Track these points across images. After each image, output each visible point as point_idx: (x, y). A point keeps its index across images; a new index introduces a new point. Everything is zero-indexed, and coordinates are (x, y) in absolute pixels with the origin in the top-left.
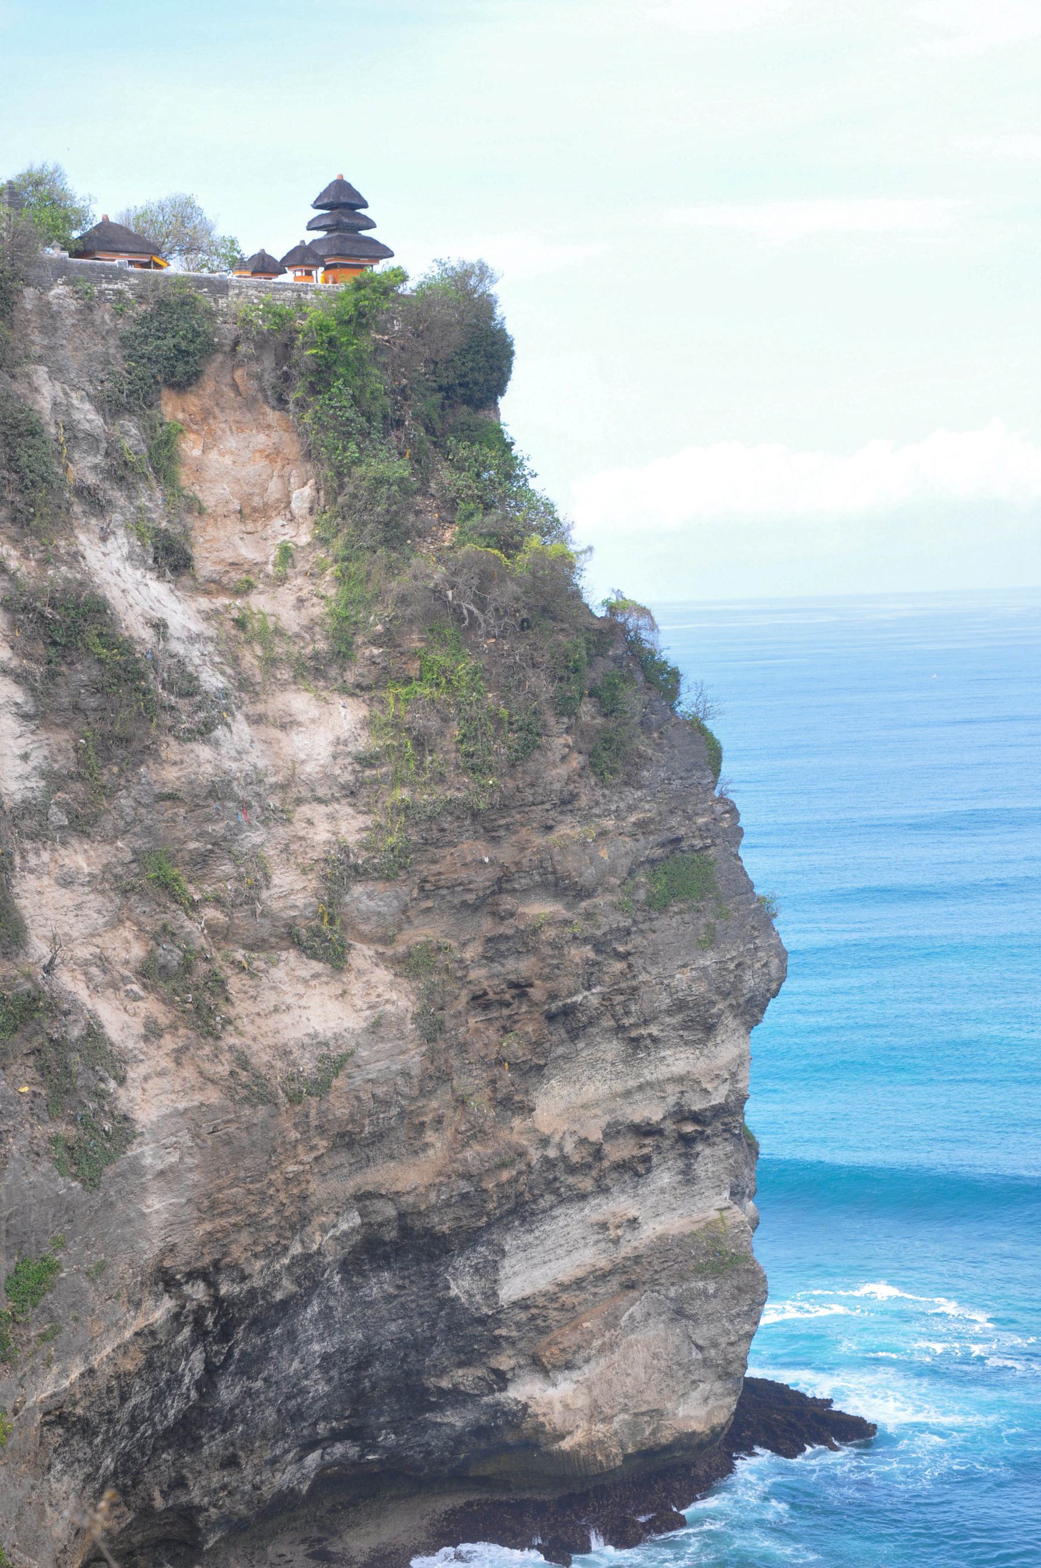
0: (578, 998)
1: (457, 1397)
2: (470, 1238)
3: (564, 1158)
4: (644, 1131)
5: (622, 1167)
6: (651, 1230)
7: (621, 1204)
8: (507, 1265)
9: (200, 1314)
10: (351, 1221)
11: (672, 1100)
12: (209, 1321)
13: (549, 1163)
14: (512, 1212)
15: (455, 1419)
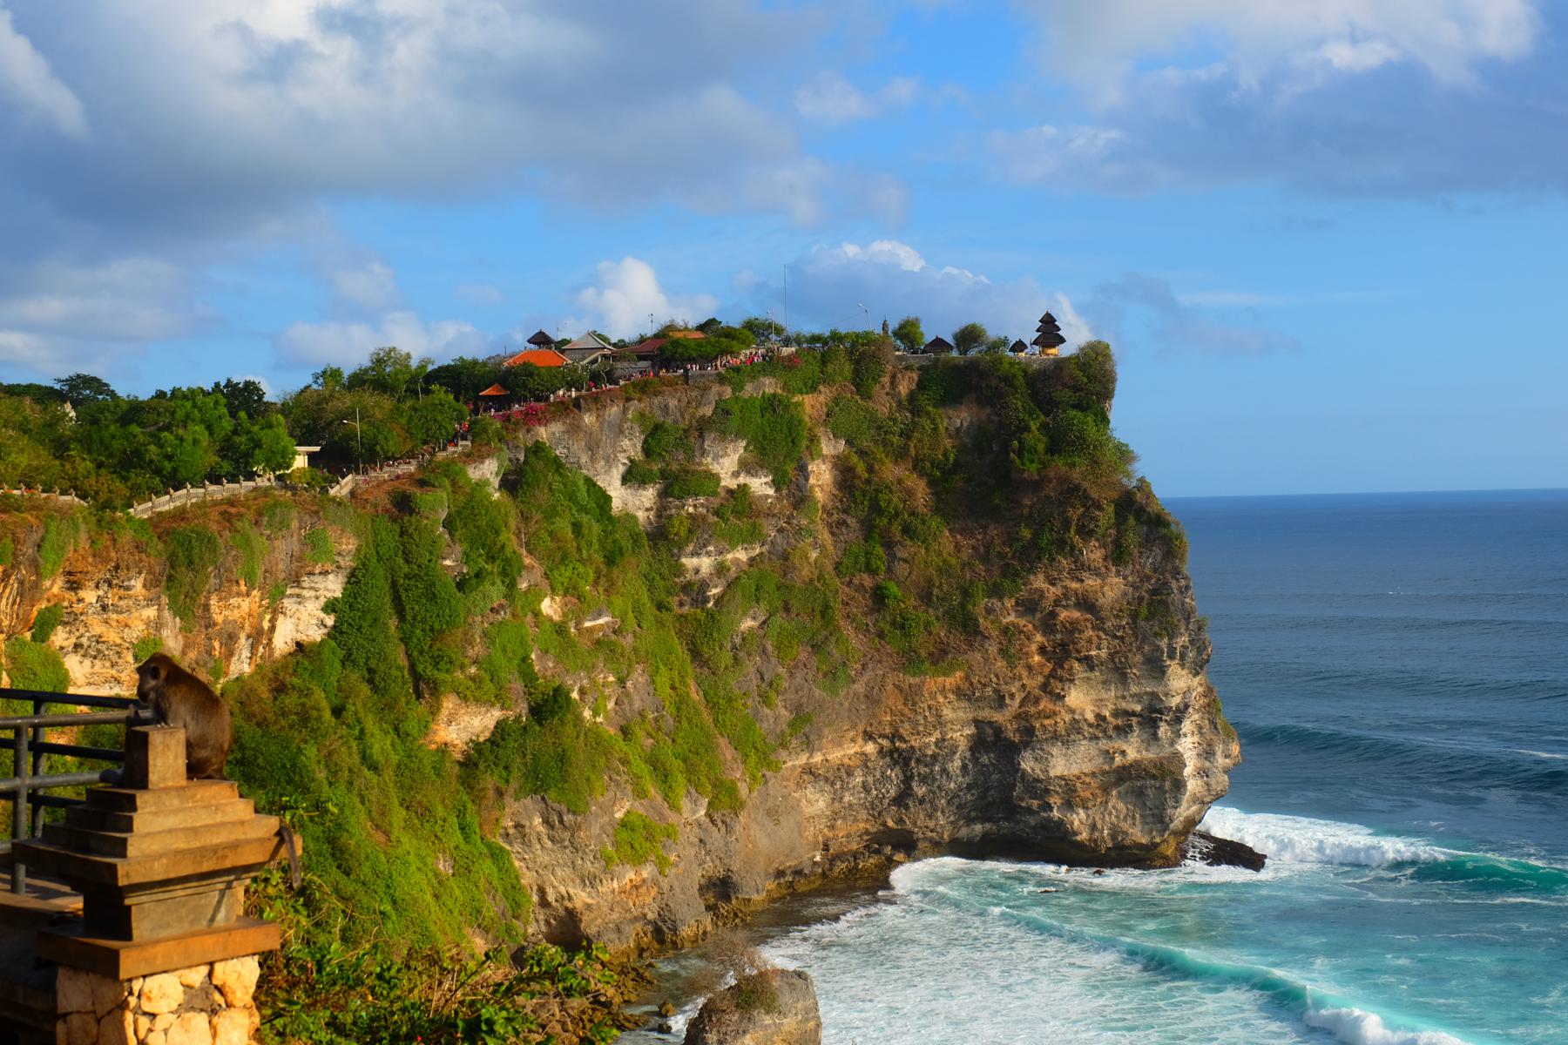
0: (1093, 653)
1: (1030, 811)
2: (1026, 745)
4: (1134, 714)
5: (1117, 728)
6: (1132, 755)
7: (1119, 744)
8: (1053, 761)
9: (891, 753)
10: (970, 731)
13: (1077, 721)
15: (1032, 821)
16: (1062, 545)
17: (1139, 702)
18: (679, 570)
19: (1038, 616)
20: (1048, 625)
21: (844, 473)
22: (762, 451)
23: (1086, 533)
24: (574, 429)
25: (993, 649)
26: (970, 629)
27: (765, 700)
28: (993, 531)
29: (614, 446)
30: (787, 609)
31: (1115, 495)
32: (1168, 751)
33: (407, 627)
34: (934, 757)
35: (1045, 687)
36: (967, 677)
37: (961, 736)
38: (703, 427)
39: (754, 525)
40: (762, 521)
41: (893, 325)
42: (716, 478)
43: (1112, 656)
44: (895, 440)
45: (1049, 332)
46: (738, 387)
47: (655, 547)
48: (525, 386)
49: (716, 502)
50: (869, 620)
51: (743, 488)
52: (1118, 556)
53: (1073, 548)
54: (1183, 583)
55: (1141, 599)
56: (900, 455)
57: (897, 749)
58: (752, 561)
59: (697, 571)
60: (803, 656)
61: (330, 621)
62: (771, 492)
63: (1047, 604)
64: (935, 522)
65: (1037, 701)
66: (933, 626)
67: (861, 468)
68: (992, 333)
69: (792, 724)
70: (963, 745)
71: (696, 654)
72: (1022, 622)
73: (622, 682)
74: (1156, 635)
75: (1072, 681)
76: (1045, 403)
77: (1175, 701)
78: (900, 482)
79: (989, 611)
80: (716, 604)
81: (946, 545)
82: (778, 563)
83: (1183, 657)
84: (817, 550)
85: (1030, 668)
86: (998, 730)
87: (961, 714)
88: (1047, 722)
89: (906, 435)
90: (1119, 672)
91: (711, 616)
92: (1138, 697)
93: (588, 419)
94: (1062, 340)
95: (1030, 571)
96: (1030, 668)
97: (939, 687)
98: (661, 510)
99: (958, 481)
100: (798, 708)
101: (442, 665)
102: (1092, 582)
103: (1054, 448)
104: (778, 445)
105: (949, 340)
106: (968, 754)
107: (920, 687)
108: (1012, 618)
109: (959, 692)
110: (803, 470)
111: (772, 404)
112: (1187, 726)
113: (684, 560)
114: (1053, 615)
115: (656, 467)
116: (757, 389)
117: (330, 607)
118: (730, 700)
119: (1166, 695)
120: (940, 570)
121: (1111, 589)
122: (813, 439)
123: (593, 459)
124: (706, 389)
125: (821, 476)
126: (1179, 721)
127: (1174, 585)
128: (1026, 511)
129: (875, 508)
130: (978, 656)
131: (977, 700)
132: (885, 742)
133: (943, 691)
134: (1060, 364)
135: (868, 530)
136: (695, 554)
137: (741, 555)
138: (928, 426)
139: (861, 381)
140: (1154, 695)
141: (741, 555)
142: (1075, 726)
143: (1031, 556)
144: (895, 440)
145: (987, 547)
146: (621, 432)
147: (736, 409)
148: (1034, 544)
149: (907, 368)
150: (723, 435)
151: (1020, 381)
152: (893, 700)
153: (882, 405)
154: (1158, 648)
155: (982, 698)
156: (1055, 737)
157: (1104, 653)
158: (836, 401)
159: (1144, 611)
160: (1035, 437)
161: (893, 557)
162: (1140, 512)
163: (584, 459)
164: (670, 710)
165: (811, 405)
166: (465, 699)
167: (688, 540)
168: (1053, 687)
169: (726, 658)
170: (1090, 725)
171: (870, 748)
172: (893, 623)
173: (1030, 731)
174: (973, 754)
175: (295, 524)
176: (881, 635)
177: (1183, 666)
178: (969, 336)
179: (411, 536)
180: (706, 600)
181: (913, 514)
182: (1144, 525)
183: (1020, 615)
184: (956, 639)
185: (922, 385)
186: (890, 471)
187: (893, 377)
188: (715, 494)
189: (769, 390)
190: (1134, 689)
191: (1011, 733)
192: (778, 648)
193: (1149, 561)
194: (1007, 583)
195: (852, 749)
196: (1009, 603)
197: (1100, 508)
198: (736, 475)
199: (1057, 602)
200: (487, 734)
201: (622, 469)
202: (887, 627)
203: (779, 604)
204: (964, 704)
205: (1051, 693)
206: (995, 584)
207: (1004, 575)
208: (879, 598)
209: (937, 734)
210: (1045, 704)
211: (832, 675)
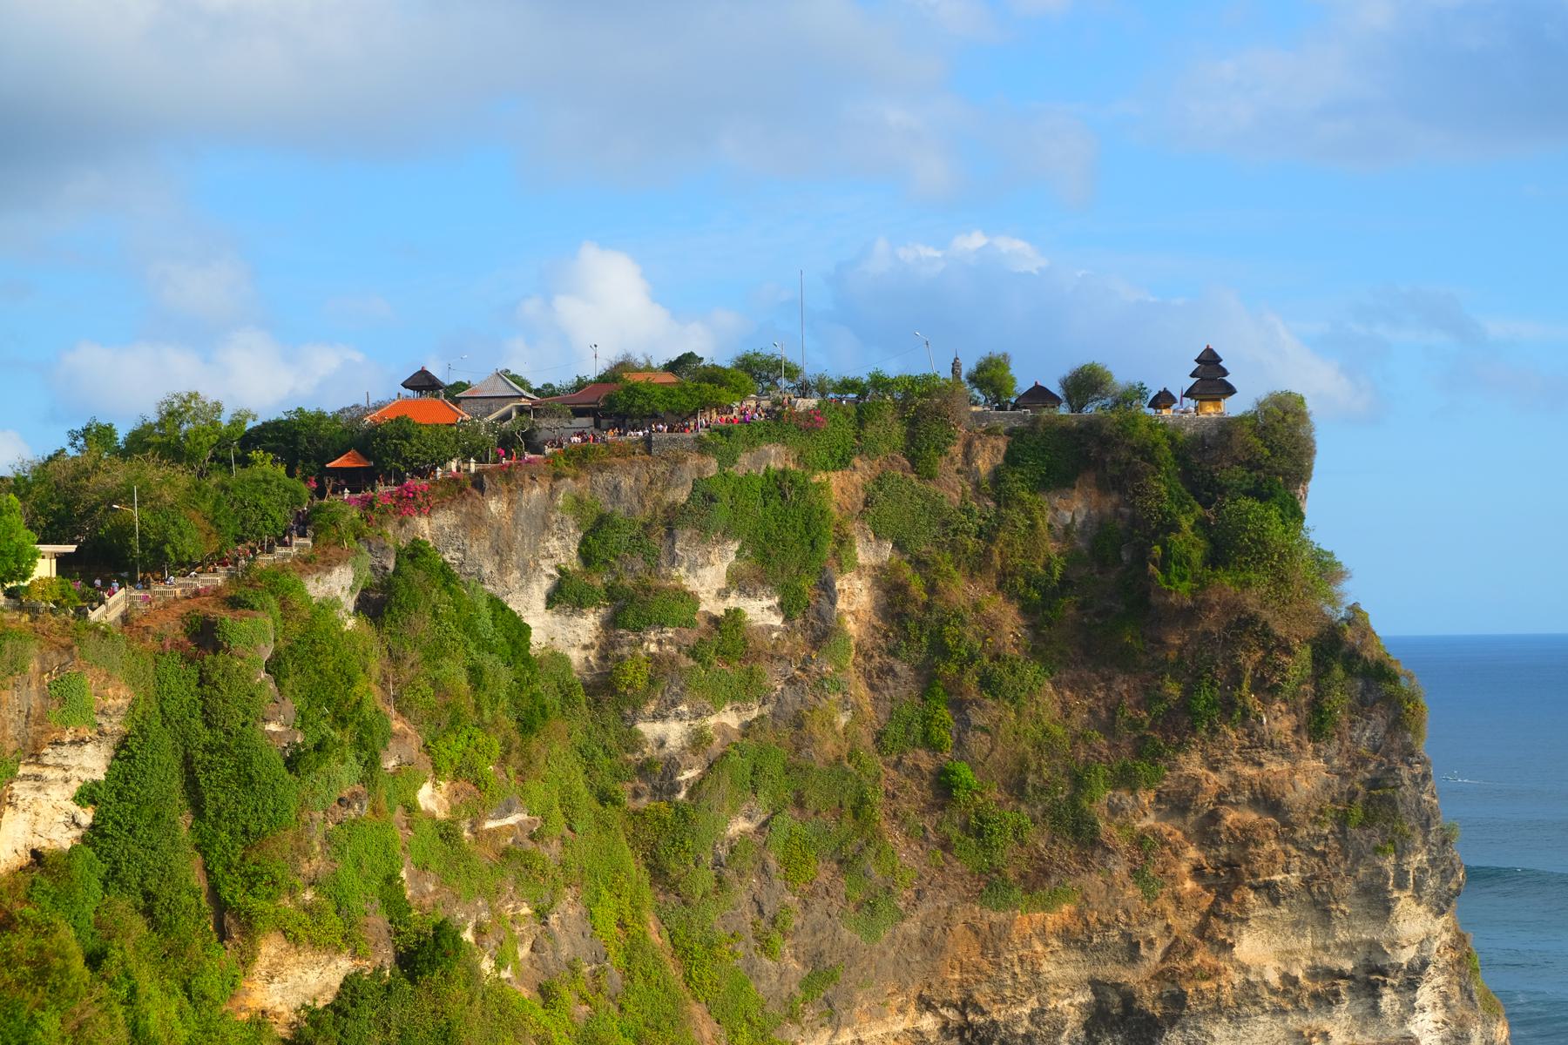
0: (1278, 878)
2: (1173, 1021)
3: (1266, 983)
4: (1341, 975)
5: (1315, 996)
7: (1318, 1021)
9: (961, 1030)
10: (1084, 997)
11: (1362, 957)
12: (968, 1035)
14: (1213, 1011)
16: (1228, 707)
17: (1350, 955)
18: (633, 741)
19: (1192, 818)
20: (1207, 831)
21: (891, 592)
22: (765, 558)
23: (1266, 689)
24: (474, 522)
25: (1120, 869)
26: (1083, 836)
27: (765, 946)
28: (1121, 685)
29: (535, 549)
30: (800, 803)
31: (1312, 631)
32: (1396, 1032)
33: (206, 827)
34: (1028, 1037)
35: (1202, 930)
36: (1080, 913)
37: (1071, 1005)
38: (672, 520)
39: (750, 673)
40: (763, 667)
41: (968, 366)
42: (692, 599)
43: (1307, 883)
44: (970, 543)
45: (1211, 377)
46: (728, 459)
47: (596, 705)
48: (397, 455)
49: (691, 636)
50: (928, 822)
51: (734, 615)
52: (1316, 725)
53: (1246, 714)
54: (1418, 769)
55: (1353, 794)
56: (978, 566)
57: (970, 1025)
58: (747, 728)
59: (661, 743)
60: (824, 877)
61: (86, 817)
62: (777, 621)
63: (1206, 801)
64: (1031, 671)
65: (1189, 952)
66: (1025, 830)
67: (917, 586)
68: (1122, 376)
69: (807, 984)
70: (1073, 1019)
71: (658, 873)
72: (1166, 828)
73: (542, 915)
74: (1377, 850)
75: (1244, 921)
76: (1204, 488)
77: (1406, 956)
78: (977, 607)
79: (1114, 810)
80: (691, 794)
81: (1045, 709)
82: (786, 733)
83: (1418, 885)
84: (846, 714)
85: (1178, 900)
86: (1128, 998)
87: (1070, 971)
88: (1205, 985)
89: (987, 535)
90: (1322, 911)
91: (682, 813)
92: (1348, 948)
93: (495, 506)
94: (1230, 390)
95: (1179, 748)
96: (1178, 900)
97: (1036, 927)
98: (607, 649)
99: (1067, 607)
100: (815, 959)
101: (260, 888)
102: (1275, 767)
103: (1218, 557)
104: (789, 548)
105: (1055, 388)
106: (1081, 1034)
107: (1006, 927)
108: (1150, 821)
109: (1067, 937)
110: (826, 588)
111: (779, 485)
112: (1425, 995)
113: (642, 726)
114: (1214, 817)
115: (598, 582)
116: (756, 462)
117: (86, 796)
118: (710, 945)
119: (1393, 945)
120: (1038, 746)
121: (1306, 777)
122: (843, 541)
123: (502, 568)
124: (679, 461)
125: (855, 598)
126: (1412, 986)
127: (1405, 772)
128: (1172, 655)
129: (940, 649)
130: (1097, 879)
131: (1095, 949)
132: (951, 1014)
133: (1042, 934)
134: (1227, 427)
135: (927, 681)
136: (659, 716)
137: (730, 719)
138: (1022, 521)
139: (918, 453)
140: (1374, 946)
141: (730, 719)
142: (1250, 993)
143: (1180, 724)
144: (970, 543)
145: (1112, 712)
146: (546, 526)
147: (724, 494)
148: (1185, 706)
149: (989, 432)
150: (704, 532)
151: (1165, 452)
152: (962, 946)
153: (951, 489)
154: (1380, 872)
155: (1103, 947)
156: (1218, 1009)
157: (1294, 878)
158: (879, 482)
159: (1357, 813)
160: (1188, 540)
161: (965, 723)
162: (1352, 659)
163: (488, 568)
164: (616, 960)
165: (839, 488)
166: (296, 940)
167: (648, 695)
168: (1214, 929)
169: (704, 879)
170: (1273, 992)
171: (928, 1023)
172: (965, 827)
173: (1178, 1000)
174: (1088, 1035)
175: (34, 665)
176: (946, 845)
177: (1418, 900)
178: (1085, 384)
179: (215, 685)
180: (675, 789)
181: (996, 657)
182: (1356, 677)
183: (1164, 816)
184: (1064, 853)
185: (1012, 459)
186: (962, 590)
187: (968, 445)
188: (689, 624)
189: (776, 465)
190: (1342, 935)
191: (1149, 1001)
192: (786, 864)
193: (1366, 734)
194: (1143, 767)
195: (899, 1024)
196: (1146, 798)
197: (1288, 651)
198: (723, 594)
199: (1221, 798)
200: (329, 997)
201: (547, 584)
202: (955, 833)
203: (789, 796)
204: (1075, 955)
205: (1211, 939)
206: (1124, 769)
207: (1138, 754)
208: (943, 787)
209: (1033, 1003)
210: (1203, 957)
211: (869, 907)
